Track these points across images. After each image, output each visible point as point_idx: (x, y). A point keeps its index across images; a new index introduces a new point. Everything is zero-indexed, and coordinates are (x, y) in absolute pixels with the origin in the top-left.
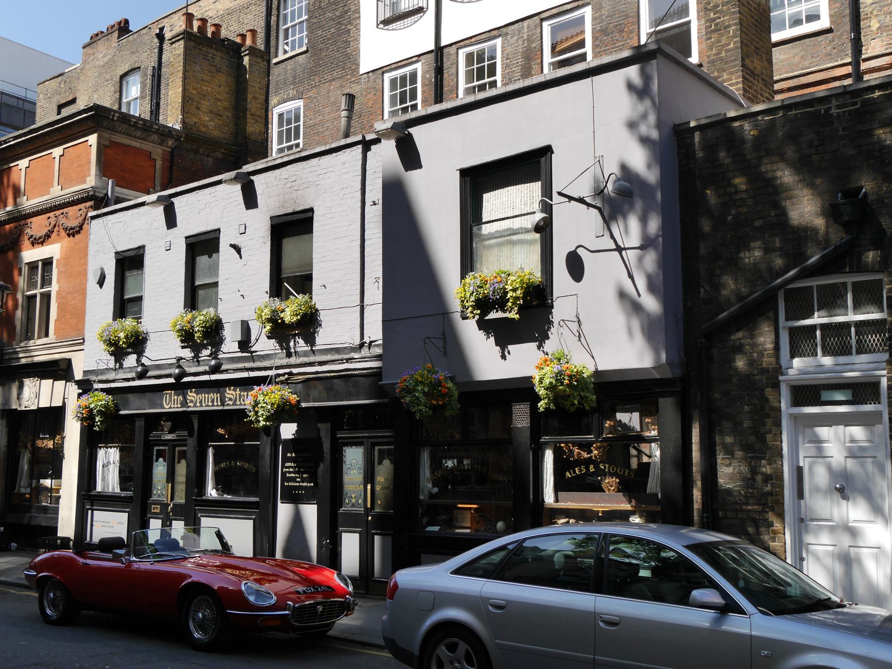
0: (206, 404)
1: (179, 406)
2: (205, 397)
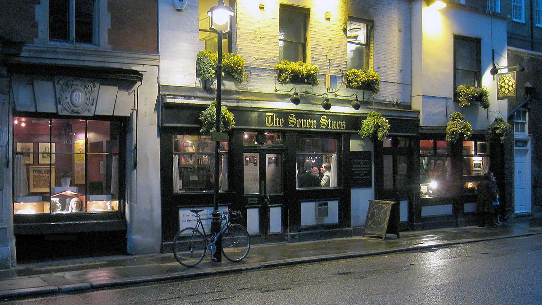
0: (305, 126)
1: (281, 126)
2: (304, 122)
